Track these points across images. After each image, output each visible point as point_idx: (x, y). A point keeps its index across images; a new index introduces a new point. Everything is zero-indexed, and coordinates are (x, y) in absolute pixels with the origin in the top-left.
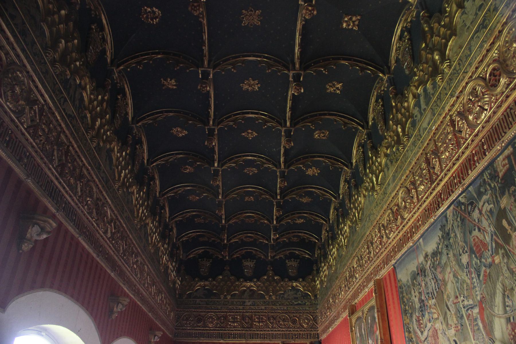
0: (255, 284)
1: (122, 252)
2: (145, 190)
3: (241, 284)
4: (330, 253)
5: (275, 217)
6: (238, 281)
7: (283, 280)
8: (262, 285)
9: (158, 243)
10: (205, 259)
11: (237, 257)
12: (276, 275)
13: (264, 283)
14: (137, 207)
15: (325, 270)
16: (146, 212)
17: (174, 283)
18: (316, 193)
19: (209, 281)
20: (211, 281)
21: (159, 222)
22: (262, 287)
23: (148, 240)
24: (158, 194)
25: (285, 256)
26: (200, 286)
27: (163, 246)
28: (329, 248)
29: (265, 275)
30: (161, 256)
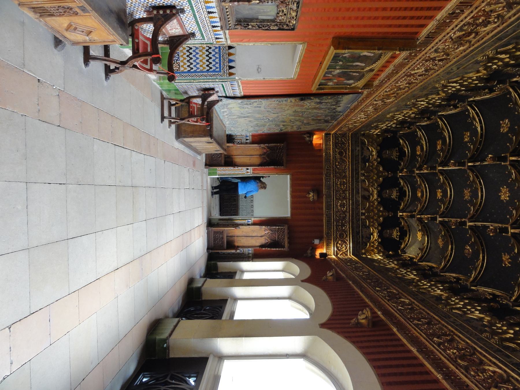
0: (375, 200)
1: (412, 73)
2: (479, 85)
3: (375, 189)
4: (409, 272)
5: (446, 219)
6: (378, 185)
7: (379, 225)
8: (375, 206)
9: (416, 108)
10: (398, 154)
11: (400, 183)
12: (384, 219)
13: (376, 208)
14: (460, 80)
15: (390, 264)
16: (453, 91)
17: (376, 128)
18: (477, 261)
19: (377, 159)
20: (377, 161)
21: (440, 106)
22: (372, 206)
23: (419, 97)
24: (472, 99)
25: (403, 227)
26: (372, 151)
27: (413, 113)
28: (415, 270)
29: (384, 208)
30: (403, 113)
